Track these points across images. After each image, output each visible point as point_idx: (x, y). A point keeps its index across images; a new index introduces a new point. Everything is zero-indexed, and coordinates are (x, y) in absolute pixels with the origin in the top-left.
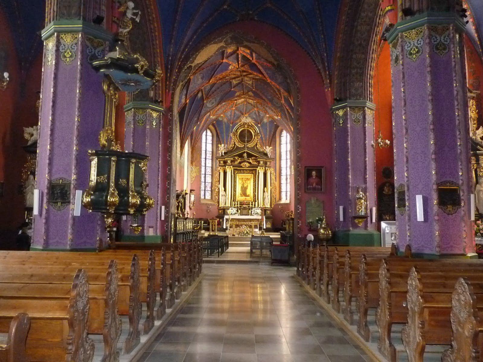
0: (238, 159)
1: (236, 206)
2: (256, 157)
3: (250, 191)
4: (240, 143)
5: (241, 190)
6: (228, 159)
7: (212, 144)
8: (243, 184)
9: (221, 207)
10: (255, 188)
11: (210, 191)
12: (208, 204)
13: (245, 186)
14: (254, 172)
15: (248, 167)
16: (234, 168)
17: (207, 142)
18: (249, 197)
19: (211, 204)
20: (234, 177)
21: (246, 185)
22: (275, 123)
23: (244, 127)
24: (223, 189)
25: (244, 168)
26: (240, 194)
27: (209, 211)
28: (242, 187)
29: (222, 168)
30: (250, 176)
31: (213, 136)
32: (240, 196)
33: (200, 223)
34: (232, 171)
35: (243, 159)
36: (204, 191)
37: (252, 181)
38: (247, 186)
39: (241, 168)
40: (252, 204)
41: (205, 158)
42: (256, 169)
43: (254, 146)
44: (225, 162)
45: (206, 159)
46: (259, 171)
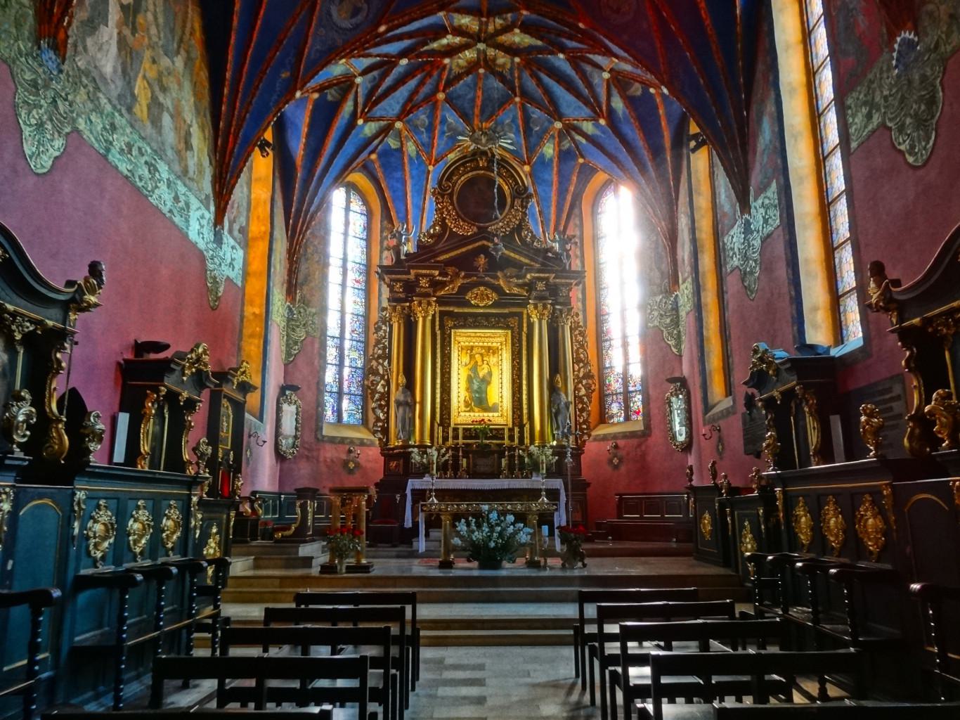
0: (457, 275)
1: (450, 441)
2: (519, 265)
3: (500, 392)
4: (464, 221)
5: (467, 390)
6: (424, 272)
7: (368, 240)
8: (474, 369)
9: (397, 447)
10: (520, 377)
11: (358, 398)
12: (352, 441)
13: (482, 373)
14: (513, 322)
15: (490, 307)
16: (443, 309)
17: (351, 232)
18: (496, 414)
19: (362, 443)
20: (443, 340)
21: (486, 371)
22: (581, 161)
23: (478, 168)
24: (402, 380)
25: (478, 307)
26: (465, 401)
27: (352, 465)
28: (470, 380)
29: (399, 308)
30: (498, 338)
31: (369, 214)
32: (463, 409)
33: (298, 510)
34: (434, 316)
35: (476, 276)
36: (335, 396)
37: (506, 356)
38: (490, 374)
39: (466, 310)
40: (511, 438)
41: (340, 281)
42: (520, 315)
43: (512, 232)
44: (410, 289)
45: (343, 285)
46: (535, 320)
